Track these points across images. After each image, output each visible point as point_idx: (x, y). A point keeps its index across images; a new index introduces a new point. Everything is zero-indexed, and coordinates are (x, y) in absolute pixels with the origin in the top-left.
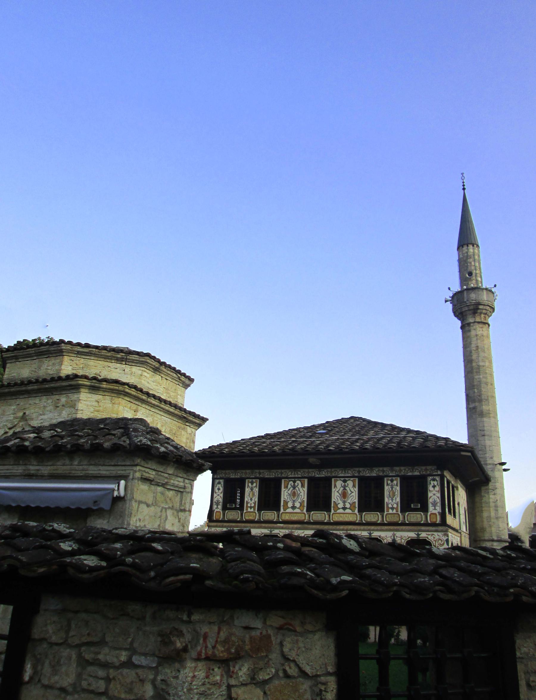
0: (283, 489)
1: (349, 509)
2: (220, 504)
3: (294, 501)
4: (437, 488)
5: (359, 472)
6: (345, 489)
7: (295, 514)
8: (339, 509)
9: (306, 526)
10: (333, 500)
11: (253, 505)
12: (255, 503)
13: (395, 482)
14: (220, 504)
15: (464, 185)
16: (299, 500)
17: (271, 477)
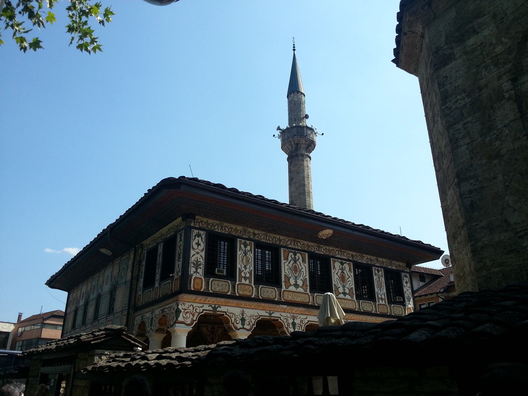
0: (283, 261)
1: (348, 294)
2: (202, 266)
3: (296, 277)
4: (409, 285)
5: (353, 256)
6: (343, 272)
7: (299, 294)
8: (340, 293)
9: (311, 310)
10: (334, 283)
11: (248, 275)
12: (250, 273)
13: (380, 272)
14: (202, 266)
15: (294, 47)
16: (301, 278)
17: (268, 242)
